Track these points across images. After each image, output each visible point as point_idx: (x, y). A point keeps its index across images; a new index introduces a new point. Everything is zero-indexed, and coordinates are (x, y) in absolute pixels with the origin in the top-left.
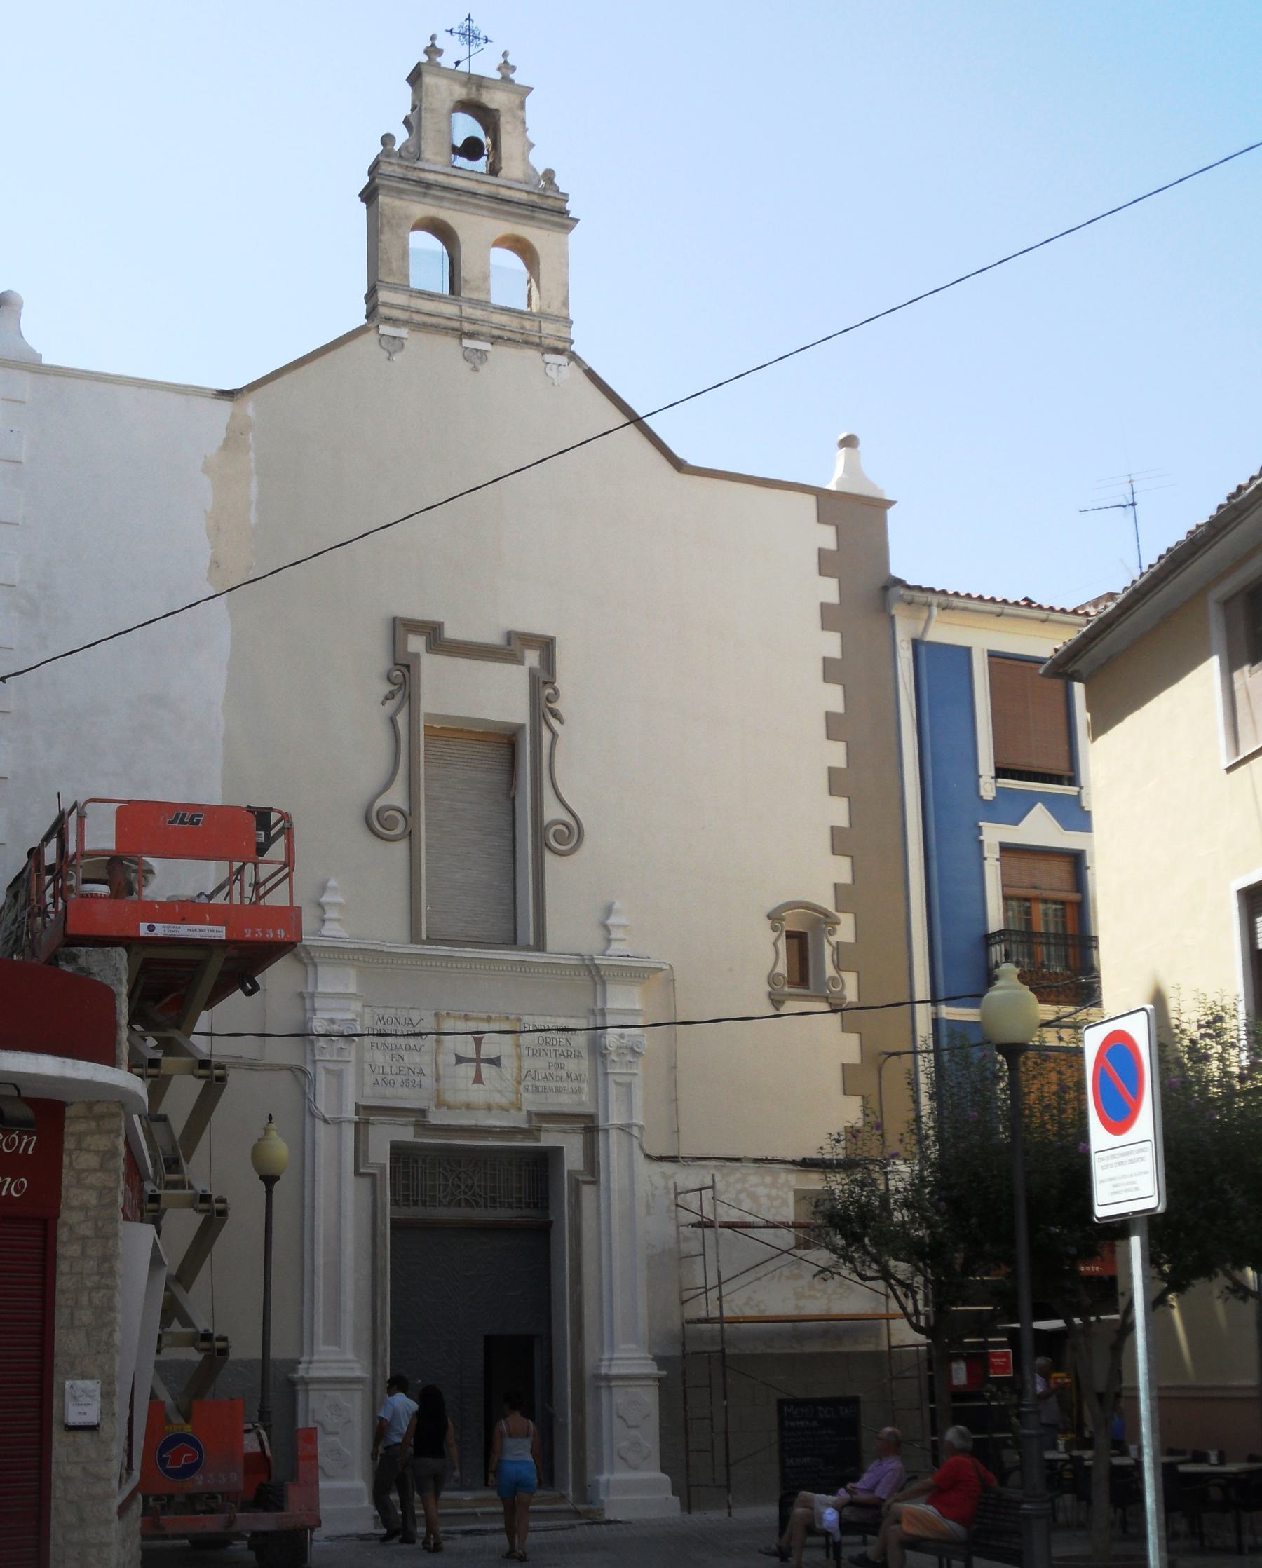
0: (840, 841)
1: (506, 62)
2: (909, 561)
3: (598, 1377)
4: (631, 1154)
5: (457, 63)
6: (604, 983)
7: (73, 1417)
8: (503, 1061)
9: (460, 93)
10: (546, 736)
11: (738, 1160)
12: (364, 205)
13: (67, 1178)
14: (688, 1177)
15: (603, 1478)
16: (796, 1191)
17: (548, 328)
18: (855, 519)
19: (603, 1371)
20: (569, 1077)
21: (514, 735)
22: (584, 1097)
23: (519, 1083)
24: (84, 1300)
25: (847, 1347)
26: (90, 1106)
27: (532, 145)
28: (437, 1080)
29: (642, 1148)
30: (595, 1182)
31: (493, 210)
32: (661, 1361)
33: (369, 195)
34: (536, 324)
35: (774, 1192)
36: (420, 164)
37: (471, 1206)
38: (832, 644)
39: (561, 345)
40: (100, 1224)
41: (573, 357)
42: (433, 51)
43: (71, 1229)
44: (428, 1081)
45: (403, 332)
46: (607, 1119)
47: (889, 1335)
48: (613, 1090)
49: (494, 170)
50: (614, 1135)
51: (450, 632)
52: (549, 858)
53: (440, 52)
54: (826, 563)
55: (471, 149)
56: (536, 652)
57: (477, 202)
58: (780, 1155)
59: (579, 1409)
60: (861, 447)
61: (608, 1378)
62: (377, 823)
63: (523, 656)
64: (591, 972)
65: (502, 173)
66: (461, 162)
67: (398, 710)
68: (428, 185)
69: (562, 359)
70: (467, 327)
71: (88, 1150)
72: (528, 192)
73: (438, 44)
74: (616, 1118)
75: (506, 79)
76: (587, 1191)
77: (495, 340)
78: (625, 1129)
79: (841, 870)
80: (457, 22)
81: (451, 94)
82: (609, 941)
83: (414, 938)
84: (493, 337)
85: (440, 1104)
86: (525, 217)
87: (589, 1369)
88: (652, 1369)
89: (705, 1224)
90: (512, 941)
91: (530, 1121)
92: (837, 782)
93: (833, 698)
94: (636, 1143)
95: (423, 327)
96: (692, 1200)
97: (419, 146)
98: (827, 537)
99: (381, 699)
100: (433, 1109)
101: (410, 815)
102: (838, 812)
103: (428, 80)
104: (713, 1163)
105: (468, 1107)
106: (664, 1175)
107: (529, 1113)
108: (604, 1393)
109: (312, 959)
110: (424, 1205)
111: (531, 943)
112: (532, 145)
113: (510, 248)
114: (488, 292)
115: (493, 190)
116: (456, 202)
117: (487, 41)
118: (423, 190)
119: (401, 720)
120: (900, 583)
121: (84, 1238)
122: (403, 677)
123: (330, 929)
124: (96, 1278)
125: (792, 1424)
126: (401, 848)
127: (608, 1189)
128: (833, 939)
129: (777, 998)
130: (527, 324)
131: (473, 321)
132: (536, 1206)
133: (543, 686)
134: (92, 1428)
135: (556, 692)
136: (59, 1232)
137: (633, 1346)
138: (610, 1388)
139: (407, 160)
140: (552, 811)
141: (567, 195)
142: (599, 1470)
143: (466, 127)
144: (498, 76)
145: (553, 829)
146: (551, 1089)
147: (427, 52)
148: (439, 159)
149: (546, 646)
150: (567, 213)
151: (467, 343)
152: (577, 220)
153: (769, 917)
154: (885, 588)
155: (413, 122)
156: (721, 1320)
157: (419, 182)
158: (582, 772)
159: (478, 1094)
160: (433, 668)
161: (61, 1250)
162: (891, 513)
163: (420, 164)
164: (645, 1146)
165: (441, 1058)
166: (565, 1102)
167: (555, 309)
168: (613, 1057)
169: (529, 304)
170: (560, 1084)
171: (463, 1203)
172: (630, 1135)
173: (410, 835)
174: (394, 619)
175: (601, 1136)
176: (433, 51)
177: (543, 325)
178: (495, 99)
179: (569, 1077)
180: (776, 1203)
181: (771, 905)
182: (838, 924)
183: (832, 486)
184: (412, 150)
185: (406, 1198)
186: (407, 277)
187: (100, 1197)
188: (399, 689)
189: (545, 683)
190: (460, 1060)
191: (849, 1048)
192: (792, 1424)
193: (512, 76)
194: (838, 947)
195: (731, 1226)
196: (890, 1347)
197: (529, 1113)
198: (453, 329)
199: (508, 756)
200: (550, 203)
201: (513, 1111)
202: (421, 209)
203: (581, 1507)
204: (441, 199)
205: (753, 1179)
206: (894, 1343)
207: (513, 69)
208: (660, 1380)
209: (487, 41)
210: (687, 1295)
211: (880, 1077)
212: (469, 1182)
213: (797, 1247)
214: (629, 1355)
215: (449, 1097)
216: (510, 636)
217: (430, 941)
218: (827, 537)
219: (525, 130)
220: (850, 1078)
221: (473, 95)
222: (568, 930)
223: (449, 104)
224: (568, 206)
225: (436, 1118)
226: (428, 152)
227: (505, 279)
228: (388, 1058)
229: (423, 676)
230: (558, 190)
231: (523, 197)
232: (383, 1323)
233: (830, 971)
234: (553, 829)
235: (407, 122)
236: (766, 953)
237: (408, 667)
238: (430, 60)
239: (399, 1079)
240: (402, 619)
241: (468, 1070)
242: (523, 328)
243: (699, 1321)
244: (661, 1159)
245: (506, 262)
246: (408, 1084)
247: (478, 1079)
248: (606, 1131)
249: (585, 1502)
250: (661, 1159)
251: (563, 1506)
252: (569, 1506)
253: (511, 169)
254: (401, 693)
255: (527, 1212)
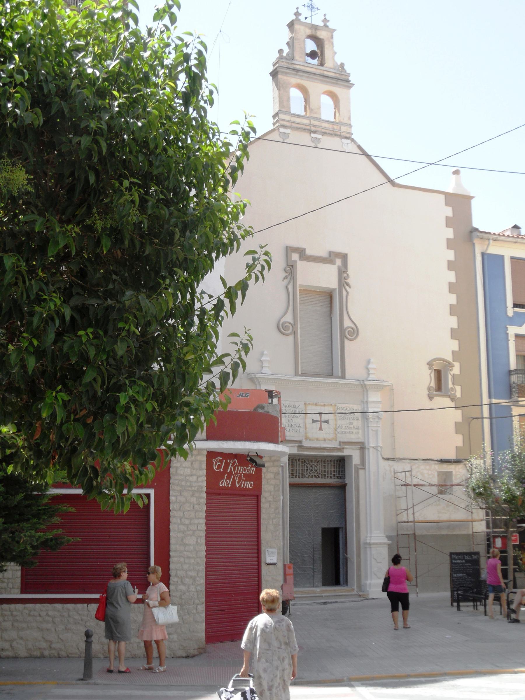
0: (454, 334)
1: (325, 18)
2: (479, 222)
3: (366, 544)
4: (378, 458)
5: (306, 18)
6: (367, 391)
7: (268, 561)
8: (330, 422)
9: (308, 32)
10: (344, 293)
11: (416, 460)
12: (271, 78)
13: (264, 481)
14: (399, 467)
15: (368, 582)
16: (438, 472)
17: (343, 129)
18: (459, 204)
19: (368, 541)
20: (354, 427)
21: (331, 292)
22: (360, 436)
23: (336, 430)
24: (271, 522)
25: (457, 532)
26: (270, 457)
27: (336, 53)
28: (305, 429)
29: (381, 455)
30: (364, 469)
31: (322, 81)
32: (389, 538)
33: (274, 74)
34: (339, 127)
35: (430, 472)
36: (294, 62)
37: (316, 478)
38: (450, 255)
39: (348, 135)
40: (275, 497)
41: (353, 140)
42: (297, 14)
43: (266, 498)
44: (302, 430)
45: (288, 131)
46: (368, 444)
47: (472, 528)
48: (371, 433)
49: (322, 64)
50: (371, 450)
51: (308, 252)
52: (346, 342)
53: (300, 14)
54: (449, 222)
55: (313, 55)
56: (339, 259)
57: (316, 77)
58: (432, 458)
59: (359, 556)
60: (461, 174)
61: (370, 544)
62: (282, 328)
63: (335, 261)
64: (362, 387)
65: (325, 65)
66: (309, 60)
67: (289, 283)
68: (298, 71)
69: (349, 141)
70: (313, 129)
71: (270, 472)
72: (335, 73)
73: (300, 11)
74: (372, 444)
75: (326, 26)
76: (361, 472)
77: (324, 134)
78: (376, 448)
79: (455, 345)
80: (306, 1)
81: (305, 33)
82: (369, 374)
83: (297, 374)
84: (323, 133)
85: (307, 438)
86: (333, 83)
87: (362, 541)
88: (386, 541)
89: (406, 485)
90: (331, 375)
91: (340, 445)
92: (453, 310)
93: (451, 277)
94: (379, 453)
95: (297, 129)
96: (401, 476)
97: (293, 54)
98: (449, 212)
99: (282, 279)
100: (304, 440)
101: (294, 325)
102: (453, 322)
103: (297, 27)
104: (408, 461)
105: (317, 439)
106: (389, 466)
107: (340, 442)
108: (368, 549)
109: (259, 382)
110: (299, 477)
111: (340, 375)
112: (336, 53)
113: (327, 95)
114: (320, 114)
115: (322, 72)
116: (308, 77)
117: (318, 9)
118: (295, 73)
119: (290, 287)
120: (476, 230)
121: (270, 501)
122: (290, 270)
123: (265, 370)
124: (274, 515)
125: (455, 561)
126: (291, 338)
127: (369, 471)
128: (452, 373)
129: (431, 396)
130: (335, 127)
131: (315, 126)
132: (341, 478)
133: (343, 273)
134: (275, 564)
135: (348, 275)
136: (262, 500)
137: (378, 532)
138: (370, 547)
139: (289, 60)
140: (347, 323)
141: (349, 74)
142: (366, 579)
143: (311, 46)
144: (322, 24)
145: (347, 331)
146: (348, 432)
147: (295, 14)
148: (300, 59)
149: (344, 257)
150: (349, 81)
151: (313, 135)
152: (354, 84)
153: (428, 364)
154: (471, 232)
155: (291, 44)
156: (414, 522)
157: (294, 69)
158: (359, 307)
159: (321, 435)
160: (301, 266)
161: (262, 505)
162: (473, 201)
163: (294, 62)
164: (382, 454)
165: (307, 421)
166: (353, 438)
167: (345, 121)
168: (371, 420)
169: (335, 118)
170: (351, 430)
171: (313, 477)
172: (377, 450)
173: (294, 333)
174: (287, 247)
175: (366, 450)
176: (297, 14)
177: (341, 127)
178: (322, 34)
179: (354, 427)
180: (431, 476)
181: (429, 359)
182: (454, 366)
183: (450, 191)
184: (290, 55)
185: (293, 475)
186: (290, 108)
187: (275, 487)
188: (289, 275)
189: (344, 272)
190: (314, 421)
191: (457, 415)
192: (455, 561)
193: (328, 24)
194: (454, 376)
195: (415, 486)
196: (473, 532)
197: (340, 442)
198: (308, 130)
199: (329, 301)
200: (343, 77)
201: (334, 441)
202: (294, 80)
203: (360, 593)
204: (302, 76)
205: (422, 467)
206: (474, 531)
207: (328, 21)
208: (388, 545)
209: (318, 9)
210: (399, 512)
211: (469, 427)
212: (316, 468)
213: (438, 494)
214: (377, 535)
215: (310, 435)
216: (330, 253)
217: (303, 375)
218: (449, 212)
219: (333, 46)
220: (458, 428)
221: (314, 33)
222: (353, 369)
223: (304, 36)
224: (350, 78)
225: (305, 444)
226: (297, 57)
227: (326, 109)
228: (287, 421)
229: (298, 269)
230: (346, 72)
231: (332, 75)
232: (287, 523)
233: (451, 385)
234: (347, 331)
235: (288, 44)
236: (427, 379)
237: (292, 266)
238: (297, 18)
239: (291, 429)
240: (290, 247)
241: (317, 425)
242: (334, 129)
243: (405, 522)
244: (388, 459)
245: (326, 102)
246: (295, 431)
247: (321, 429)
248: (368, 448)
249: (361, 592)
250: (388, 459)
251: (353, 593)
252: (355, 593)
253: (329, 63)
254: (290, 277)
255: (337, 480)
